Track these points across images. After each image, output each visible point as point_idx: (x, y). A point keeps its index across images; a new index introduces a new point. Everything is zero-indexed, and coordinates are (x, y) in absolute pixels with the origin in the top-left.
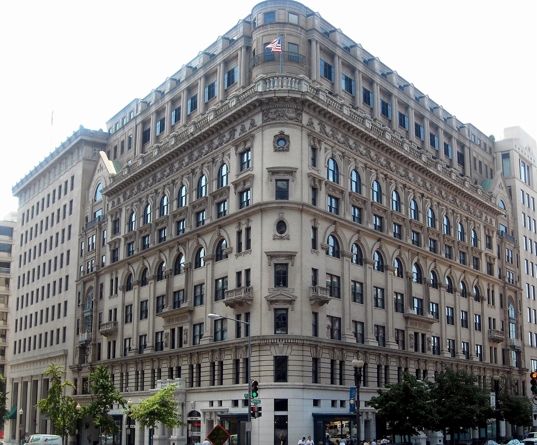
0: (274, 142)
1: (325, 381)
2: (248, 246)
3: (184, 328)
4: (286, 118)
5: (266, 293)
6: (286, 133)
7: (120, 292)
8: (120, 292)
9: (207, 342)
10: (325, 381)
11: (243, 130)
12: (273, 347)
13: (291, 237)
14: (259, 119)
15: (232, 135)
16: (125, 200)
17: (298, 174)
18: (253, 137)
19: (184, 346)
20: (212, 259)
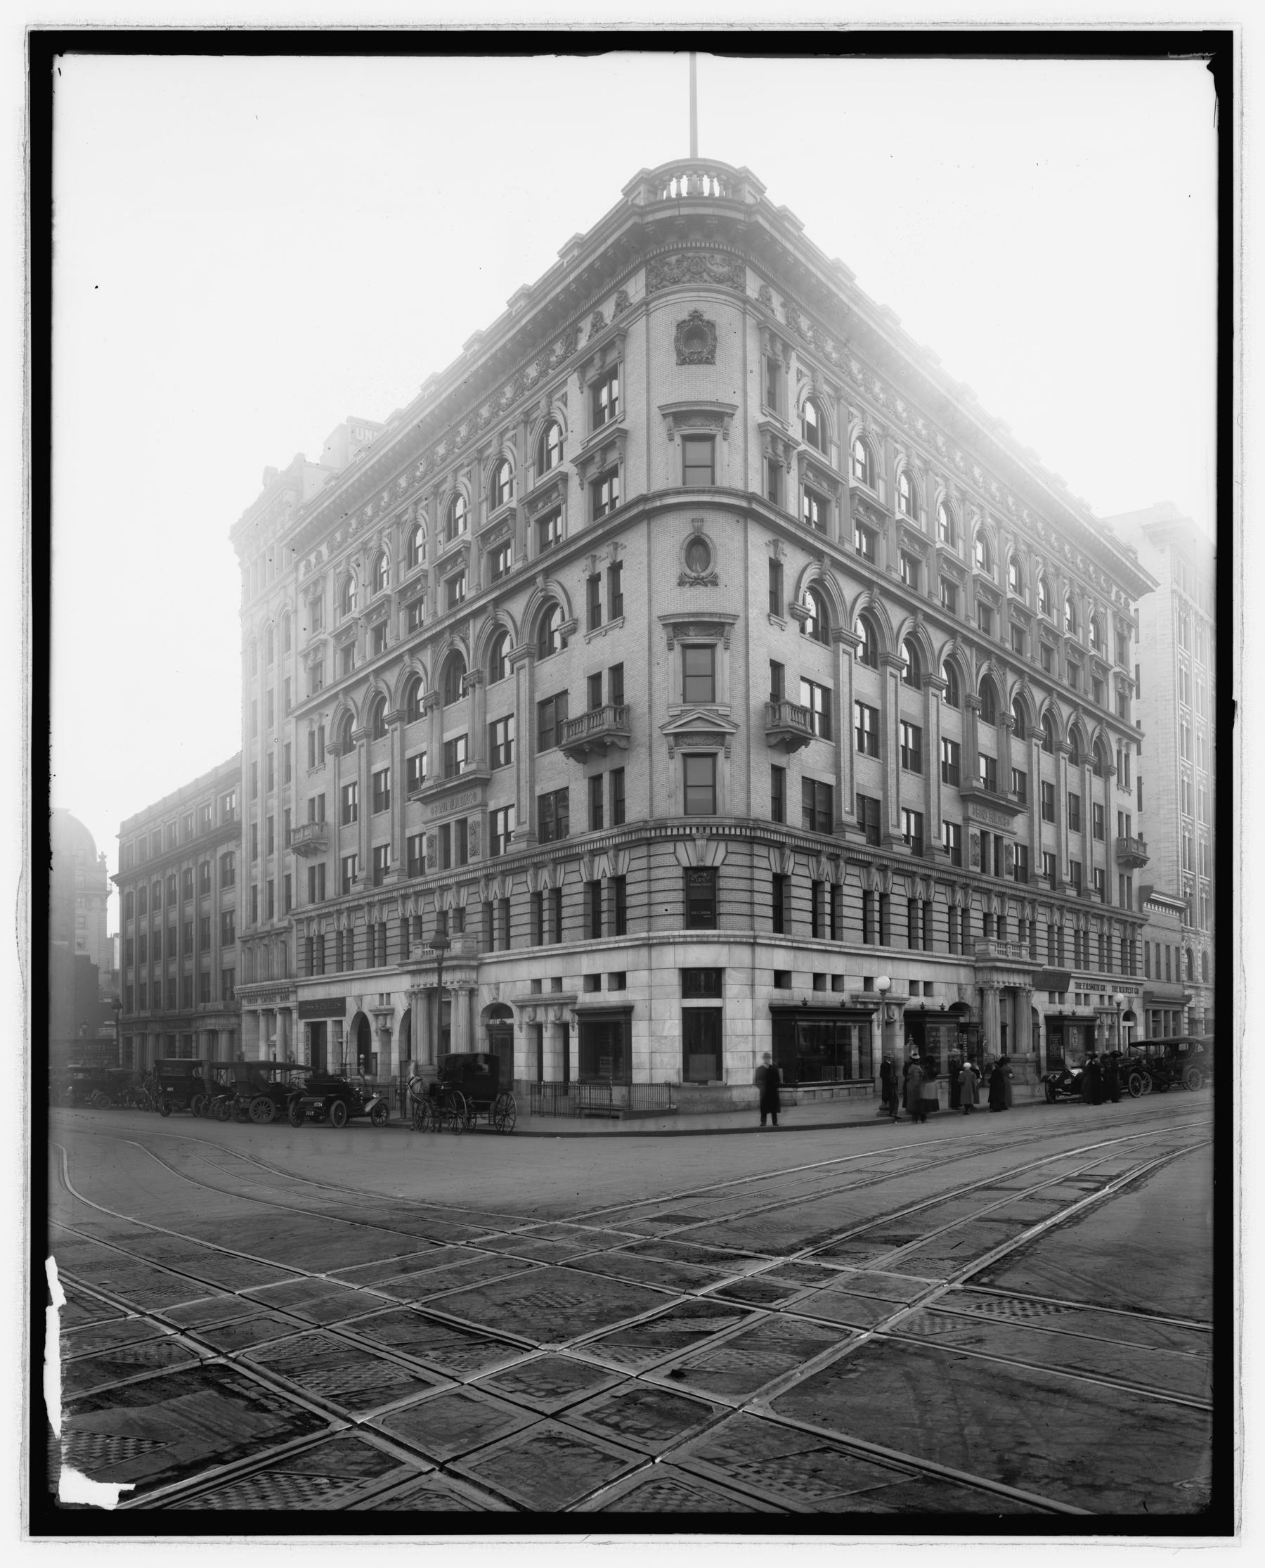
0: (677, 340)
1: (801, 930)
2: (617, 610)
3: (470, 821)
4: (705, 276)
5: (661, 716)
6: (706, 317)
7: (329, 759)
8: (329, 759)
9: (523, 846)
10: (801, 930)
11: (597, 325)
12: (680, 846)
13: (723, 580)
14: (636, 289)
15: (571, 343)
16: (331, 551)
17: (736, 425)
18: (623, 335)
19: (470, 860)
20: (529, 654)
